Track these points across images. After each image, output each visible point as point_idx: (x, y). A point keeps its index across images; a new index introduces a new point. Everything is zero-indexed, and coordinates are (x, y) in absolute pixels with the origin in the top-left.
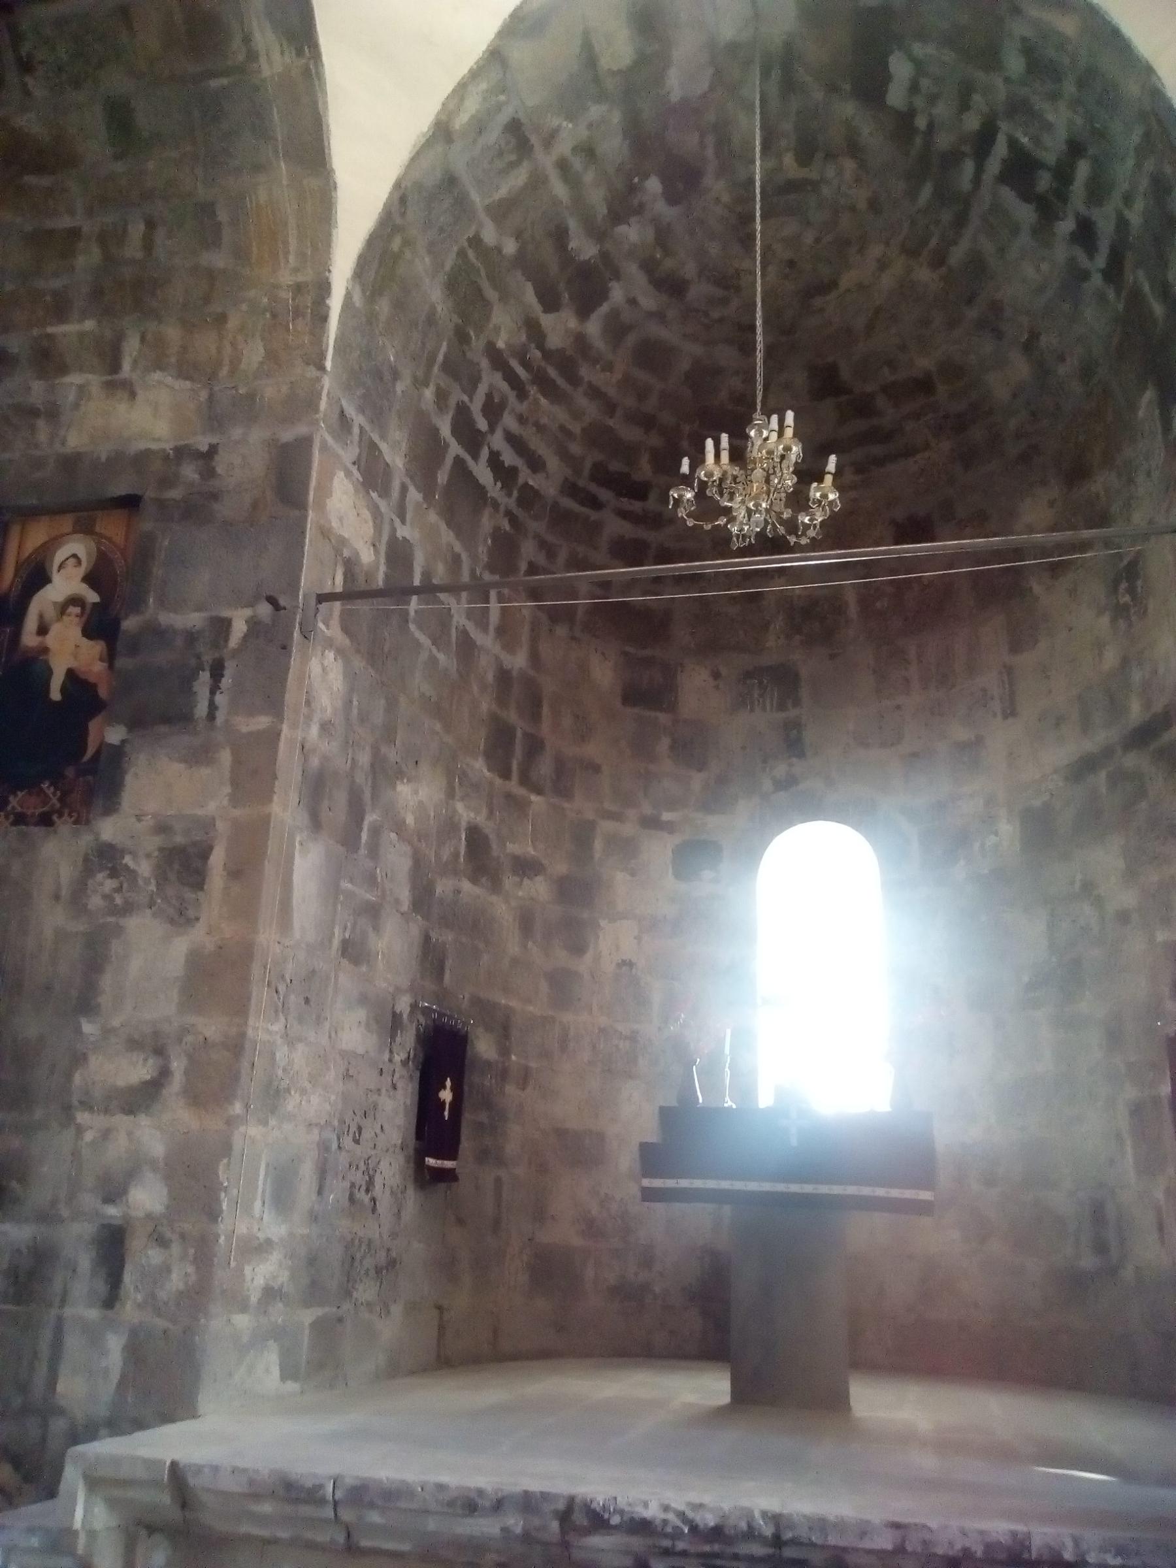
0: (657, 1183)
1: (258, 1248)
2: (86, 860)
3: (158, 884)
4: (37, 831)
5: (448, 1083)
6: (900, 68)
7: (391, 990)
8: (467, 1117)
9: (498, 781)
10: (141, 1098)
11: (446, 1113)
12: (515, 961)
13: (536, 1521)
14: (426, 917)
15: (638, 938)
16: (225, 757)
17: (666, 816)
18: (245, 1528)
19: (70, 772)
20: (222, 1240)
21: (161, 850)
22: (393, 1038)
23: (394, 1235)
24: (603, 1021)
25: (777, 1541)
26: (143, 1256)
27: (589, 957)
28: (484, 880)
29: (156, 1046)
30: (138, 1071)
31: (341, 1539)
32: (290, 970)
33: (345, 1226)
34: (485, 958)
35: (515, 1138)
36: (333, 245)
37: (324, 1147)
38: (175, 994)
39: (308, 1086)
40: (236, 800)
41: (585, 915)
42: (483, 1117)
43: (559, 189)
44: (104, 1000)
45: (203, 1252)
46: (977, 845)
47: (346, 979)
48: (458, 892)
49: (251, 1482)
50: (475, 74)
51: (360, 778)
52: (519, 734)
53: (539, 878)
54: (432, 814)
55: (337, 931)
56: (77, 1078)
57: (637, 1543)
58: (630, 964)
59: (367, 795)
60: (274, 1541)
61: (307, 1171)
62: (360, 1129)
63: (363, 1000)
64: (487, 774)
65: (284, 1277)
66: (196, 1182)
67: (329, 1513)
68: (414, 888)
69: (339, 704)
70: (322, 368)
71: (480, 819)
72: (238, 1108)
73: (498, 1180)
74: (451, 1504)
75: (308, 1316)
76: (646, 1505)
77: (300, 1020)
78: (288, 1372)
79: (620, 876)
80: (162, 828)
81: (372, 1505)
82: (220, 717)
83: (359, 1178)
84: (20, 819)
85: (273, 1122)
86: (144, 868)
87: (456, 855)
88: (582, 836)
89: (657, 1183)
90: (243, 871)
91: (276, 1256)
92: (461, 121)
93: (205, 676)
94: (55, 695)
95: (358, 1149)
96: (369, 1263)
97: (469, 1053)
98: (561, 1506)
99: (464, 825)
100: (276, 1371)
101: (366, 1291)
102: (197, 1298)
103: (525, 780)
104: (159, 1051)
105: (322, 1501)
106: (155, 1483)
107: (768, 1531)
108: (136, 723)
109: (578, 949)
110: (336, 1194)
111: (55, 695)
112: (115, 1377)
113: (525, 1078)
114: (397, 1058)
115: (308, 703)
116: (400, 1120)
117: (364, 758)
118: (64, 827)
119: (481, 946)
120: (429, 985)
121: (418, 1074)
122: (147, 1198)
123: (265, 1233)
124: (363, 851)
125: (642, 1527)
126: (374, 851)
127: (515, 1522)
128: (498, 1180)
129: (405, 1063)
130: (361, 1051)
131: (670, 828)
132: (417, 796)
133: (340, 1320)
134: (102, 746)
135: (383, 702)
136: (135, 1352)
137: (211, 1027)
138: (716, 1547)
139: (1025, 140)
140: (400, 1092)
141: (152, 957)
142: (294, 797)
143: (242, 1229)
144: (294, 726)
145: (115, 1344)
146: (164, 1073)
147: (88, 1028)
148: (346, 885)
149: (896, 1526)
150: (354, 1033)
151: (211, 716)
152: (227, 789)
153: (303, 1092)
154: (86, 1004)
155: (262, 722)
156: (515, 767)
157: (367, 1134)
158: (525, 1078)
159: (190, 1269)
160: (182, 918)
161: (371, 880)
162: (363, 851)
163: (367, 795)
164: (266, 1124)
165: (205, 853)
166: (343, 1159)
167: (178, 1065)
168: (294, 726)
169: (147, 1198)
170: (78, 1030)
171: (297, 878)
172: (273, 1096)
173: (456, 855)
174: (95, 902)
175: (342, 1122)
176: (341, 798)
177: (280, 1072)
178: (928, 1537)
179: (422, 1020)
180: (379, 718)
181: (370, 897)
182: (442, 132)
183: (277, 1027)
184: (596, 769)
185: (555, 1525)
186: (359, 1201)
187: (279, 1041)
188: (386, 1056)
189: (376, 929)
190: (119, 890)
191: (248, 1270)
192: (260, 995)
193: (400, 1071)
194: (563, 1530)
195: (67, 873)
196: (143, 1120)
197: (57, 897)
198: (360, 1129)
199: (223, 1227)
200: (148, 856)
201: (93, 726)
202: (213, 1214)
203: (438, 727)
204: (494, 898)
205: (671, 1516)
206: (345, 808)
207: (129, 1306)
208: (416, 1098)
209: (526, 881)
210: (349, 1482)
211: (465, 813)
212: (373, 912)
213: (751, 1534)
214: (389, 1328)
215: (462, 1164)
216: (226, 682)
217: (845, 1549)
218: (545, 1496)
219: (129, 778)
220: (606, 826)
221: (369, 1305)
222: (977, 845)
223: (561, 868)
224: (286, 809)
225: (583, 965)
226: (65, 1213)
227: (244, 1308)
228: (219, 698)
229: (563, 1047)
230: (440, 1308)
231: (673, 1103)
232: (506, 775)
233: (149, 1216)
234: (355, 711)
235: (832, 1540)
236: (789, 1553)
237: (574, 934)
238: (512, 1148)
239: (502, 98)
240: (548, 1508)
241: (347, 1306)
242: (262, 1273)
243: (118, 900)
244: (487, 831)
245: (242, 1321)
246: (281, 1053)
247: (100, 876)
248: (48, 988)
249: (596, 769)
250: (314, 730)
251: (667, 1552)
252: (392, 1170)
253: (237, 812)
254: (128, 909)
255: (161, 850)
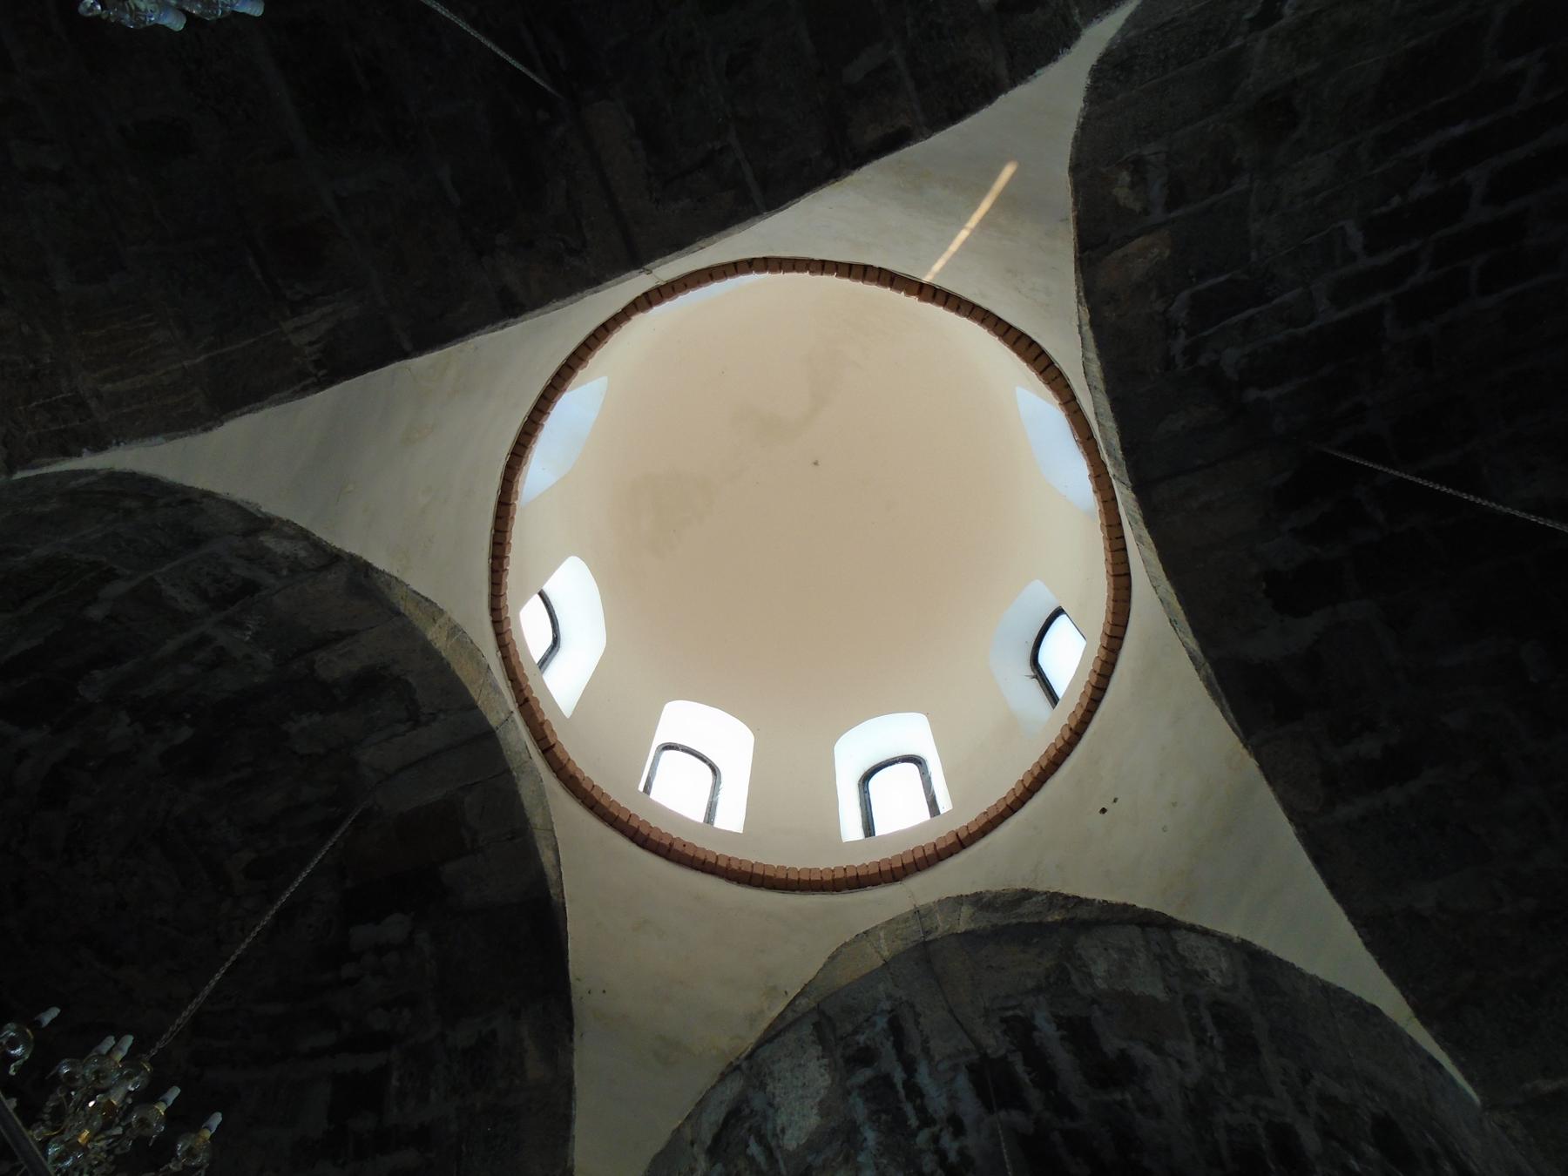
6: (394, 927)
36: (147, 442)
43: (170, 646)
50: (317, 545)
70: (11, 470)
92: (268, 540)
139: (395, 1082)
182: (256, 523)
239: (285, 572)
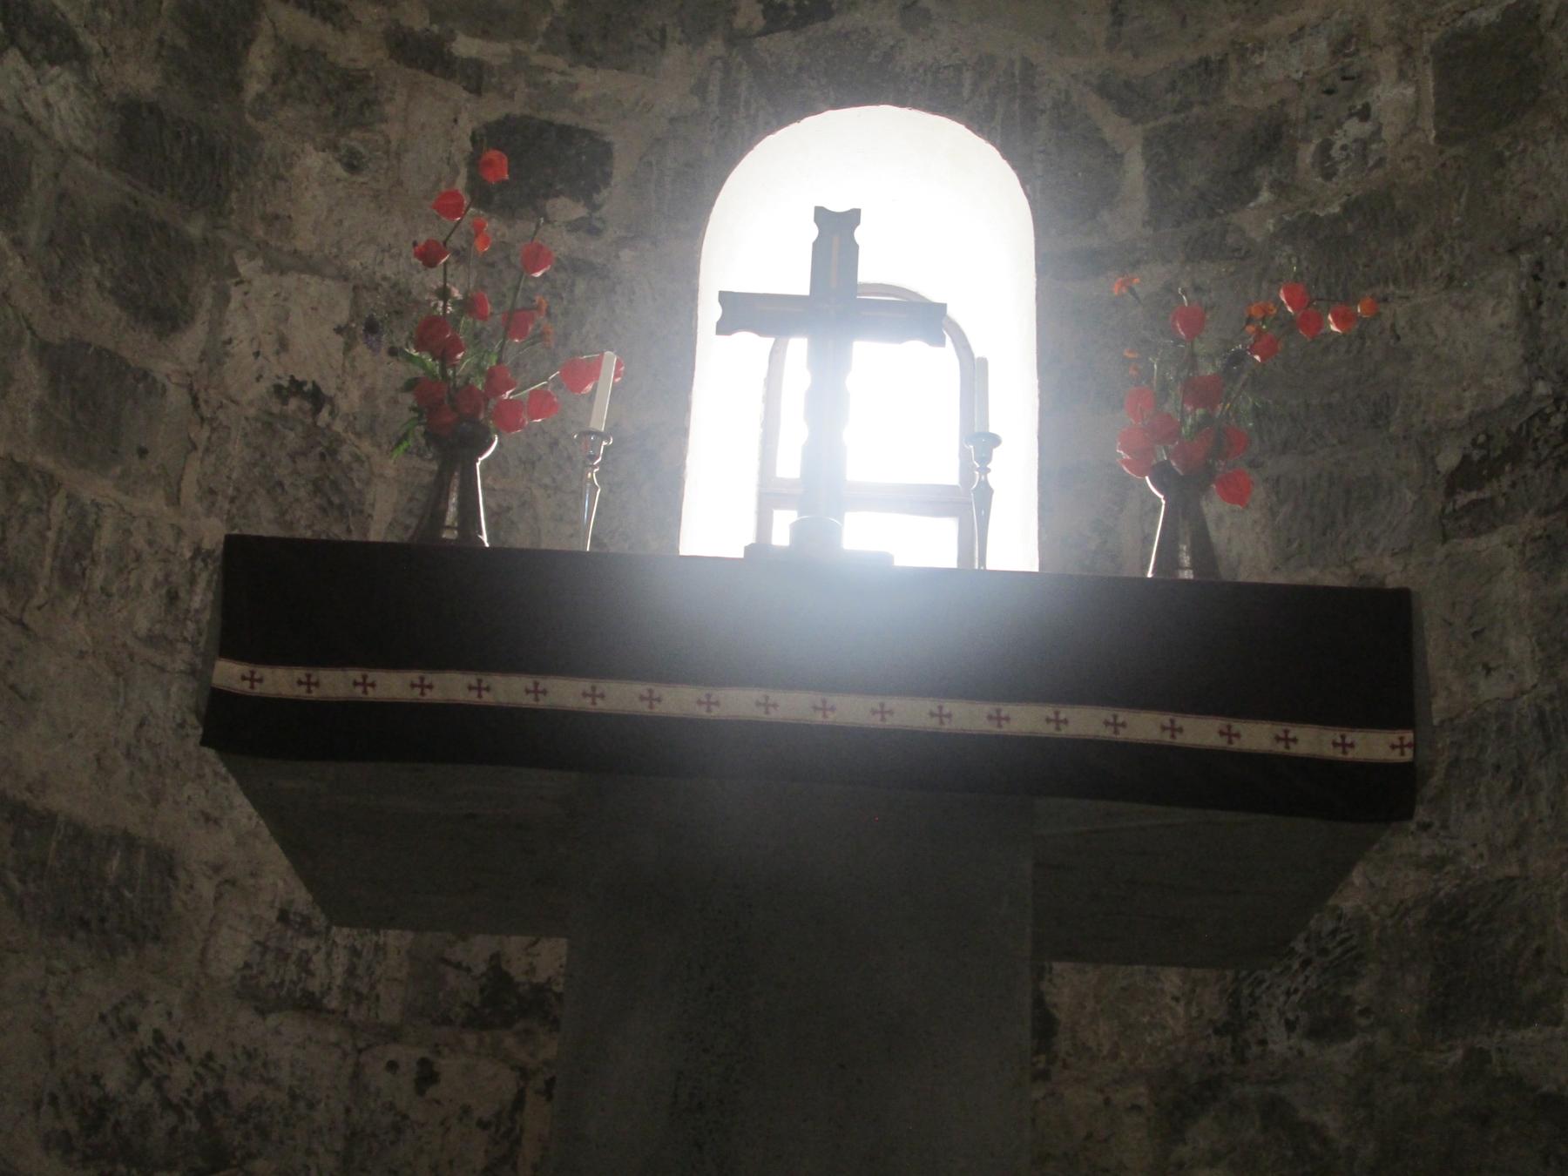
0: (280, 681)
17: (465, 46)
27: (190, 342)
46: (1307, 154)
58: (317, 398)
79: (314, 160)
89: (280, 681)
131: (476, 78)
222: (1307, 154)
223: (141, 78)
229: (69, 578)
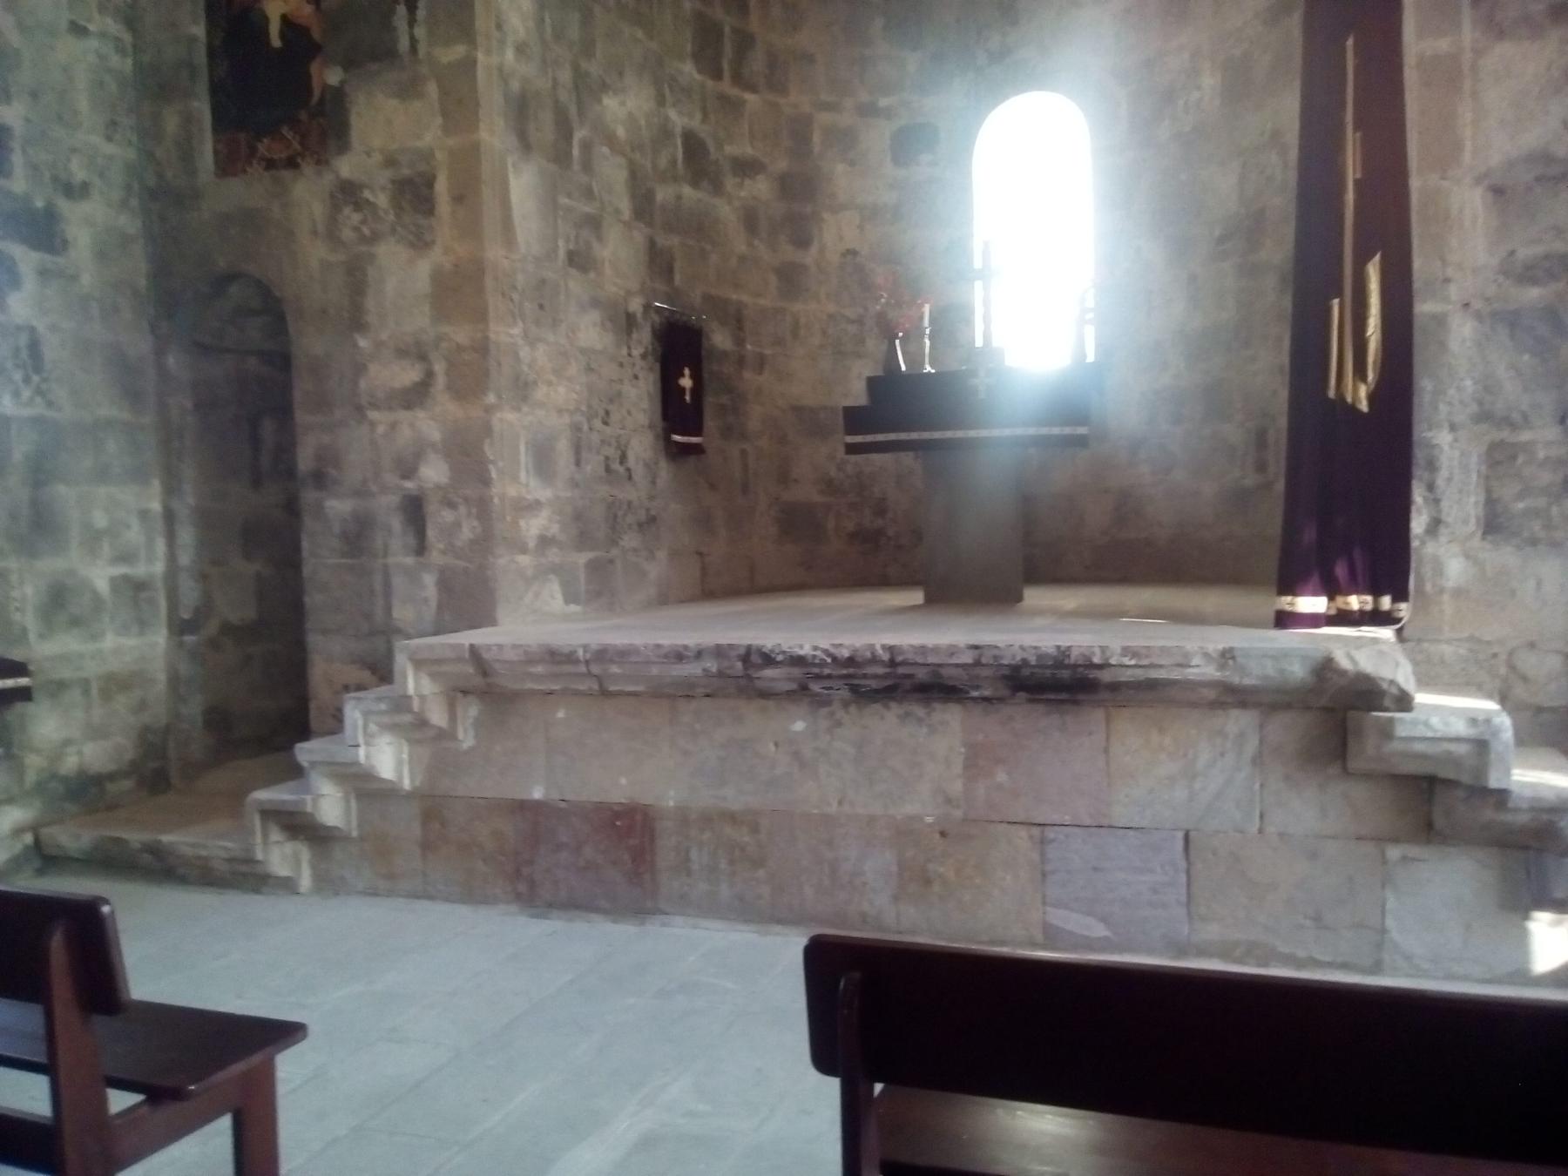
0: (859, 439)
1: (530, 507)
2: (332, 196)
3: (398, 216)
4: (286, 174)
5: (687, 371)
7: (622, 293)
8: (710, 401)
9: (710, 83)
10: (416, 396)
11: (688, 398)
12: (742, 259)
13: (726, 664)
14: (650, 224)
15: (861, 227)
16: (432, 89)
18: (530, 685)
19: (303, 116)
20: (496, 500)
21: (393, 182)
22: (629, 333)
23: (651, 498)
24: (831, 308)
25: (892, 663)
26: (439, 517)
27: (814, 250)
28: (705, 184)
29: (418, 352)
30: (408, 375)
31: (596, 687)
32: (520, 279)
33: (603, 490)
34: (714, 258)
35: (755, 417)
37: (577, 428)
38: (427, 308)
39: (553, 378)
40: (447, 130)
41: (808, 209)
42: (725, 399)
44: (371, 318)
45: (482, 508)
46: (1181, 102)
47: (576, 285)
48: (679, 197)
49: (526, 652)
51: (564, 96)
52: (727, 29)
53: (760, 177)
54: (643, 122)
55: (561, 243)
56: (363, 384)
57: (797, 672)
58: (852, 253)
59: (573, 110)
60: (550, 693)
61: (563, 446)
62: (607, 413)
63: (595, 303)
64: (698, 77)
65: (555, 529)
66: (468, 456)
67: (583, 669)
68: (633, 197)
69: (531, 24)
71: (695, 123)
72: (491, 398)
73: (744, 453)
74: (666, 656)
75: (582, 558)
76: (801, 647)
77: (537, 323)
78: (569, 598)
79: (840, 168)
80: (390, 162)
81: (612, 661)
82: (422, 50)
83: (611, 451)
84: (270, 164)
85: (525, 409)
86: (382, 200)
87: (674, 162)
88: (800, 131)
89: (859, 439)
90: (464, 195)
91: (545, 513)
93: (401, 10)
94: (276, 42)
95: (608, 430)
96: (630, 519)
97: (705, 344)
98: (742, 651)
99: (678, 130)
100: (559, 597)
101: (630, 540)
102: (484, 543)
103: (738, 79)
104: (423, 357)
105: (577, 662)
106: (459, 660)
107: (886, 657)
108: (349, 64)
109: (803, 242)
110: (593, 465)
111: (276, 42)
112: (434, 604)
113: (761, 363)
114: (636, 352)
115: (499, 27)
116: (645, 404)
117: (565, 76)
118: (308, 168)
119: (708, 247)
120: (660, 286)
121: (657, 366)
122: (434, 472)
123: (533, 499)
124: (576, 167)
125: (798, 661)
126: (587, 167)
127: (712, 665)
128: (744, 453)
129: (644, 356)
130: (599, 347)
132: (625, 107)
133: (611, 561)
134: (326, 87)
135: (577, 15)
136: (446, 584)
137: (461, 334)
138: (851, 671)
140: (641, 383)
141: (403, 277)
142: (500, 122)
143: (512, 491)
144: (488, 52)
145: (429, 580)
146: (430, 374)
147: (363, 343)
148: (564, 200)
149: (976, 647)
150: (591, 332)
151: (414, 48)
152: (439, 120)
153: (550, 384)
154: (356, 321)
155: (458, 51)
156: (726, 66)
157: (615, 417)
158: (761, 363)
159: (476, 523)
160: (420, 243)
161: (589, 194)
162: (576, 167)
163: (573, 110)
164: (518, 409)
165: (430, 183)
166: (595, 438)
167: (439, 368)
168: (488, 52)
169: (434, 472)
170: (355, 345)
171: (515, 197)
172: (522, 390)
173: (674, 162)
174: (347, 234)
175: (590, 407)
176: (547, 117)
177: (526, 369)
178: (996, 652)
179: (657, 318)
180: (574, 33)
181: (588, 209)
183: (516, 331)
184: (810, 59)
185: (739, 665)
186: (616, 469)
187: (520, 342)
188: (625, 351)
189: (600, 239)
190: (364, 222)
191: (522, 523)
192: (494, 302)
193: (640, 363)
194: (746, 669)
195: (318, 209)
196: (421, 414)
197: (315, 233)
198: (607, 413)
199: (495, 490)
200: (383, 189)
201: (314, 68)
202: (486, 482)
203: (640, 34)
204: (717, 201)
205: (818, 653)
206: (553, 128)
207: (435, 553)
208: (659, 385)
209: (747, 182)
210: (594, 647)
211: (678, 119)
212: (594, 223)
213: (874, 660)
214: (657, 568)
215: (710, 435)
216: (421, 13)
217: (940, 665)
218: (731, 646)
219: (354, 121)
220: (824, 118)
221: (635, 550)
222: (1181, 102)
223: (782, 165)
224: (494, 134)
225: (809, 257)
226: (374, 488)
227: (524, 551)
228: (420, 32)
229: (795, 335)
230: (700, 554)
231: (880, 373)
232: (717, 75)
233: (438, 487)
234: (549, 30)
235: (930, 660)
236: (901, 670)
237: (800, 231)
238: (754, 424)
240: (733, 653)
241: (615, 552)
242: (533, 527)
243: (366, 231)
244: (702, 135)
245: (524, 560)
246: (524, 353)
247: (347, 211)
248: (324, 311)
249: (810, 59)
250: (510, 55)
251: (818, 677)
252: (642, 447)
253: (451, 142)
254: (375, 238)
255: (393, 182)
